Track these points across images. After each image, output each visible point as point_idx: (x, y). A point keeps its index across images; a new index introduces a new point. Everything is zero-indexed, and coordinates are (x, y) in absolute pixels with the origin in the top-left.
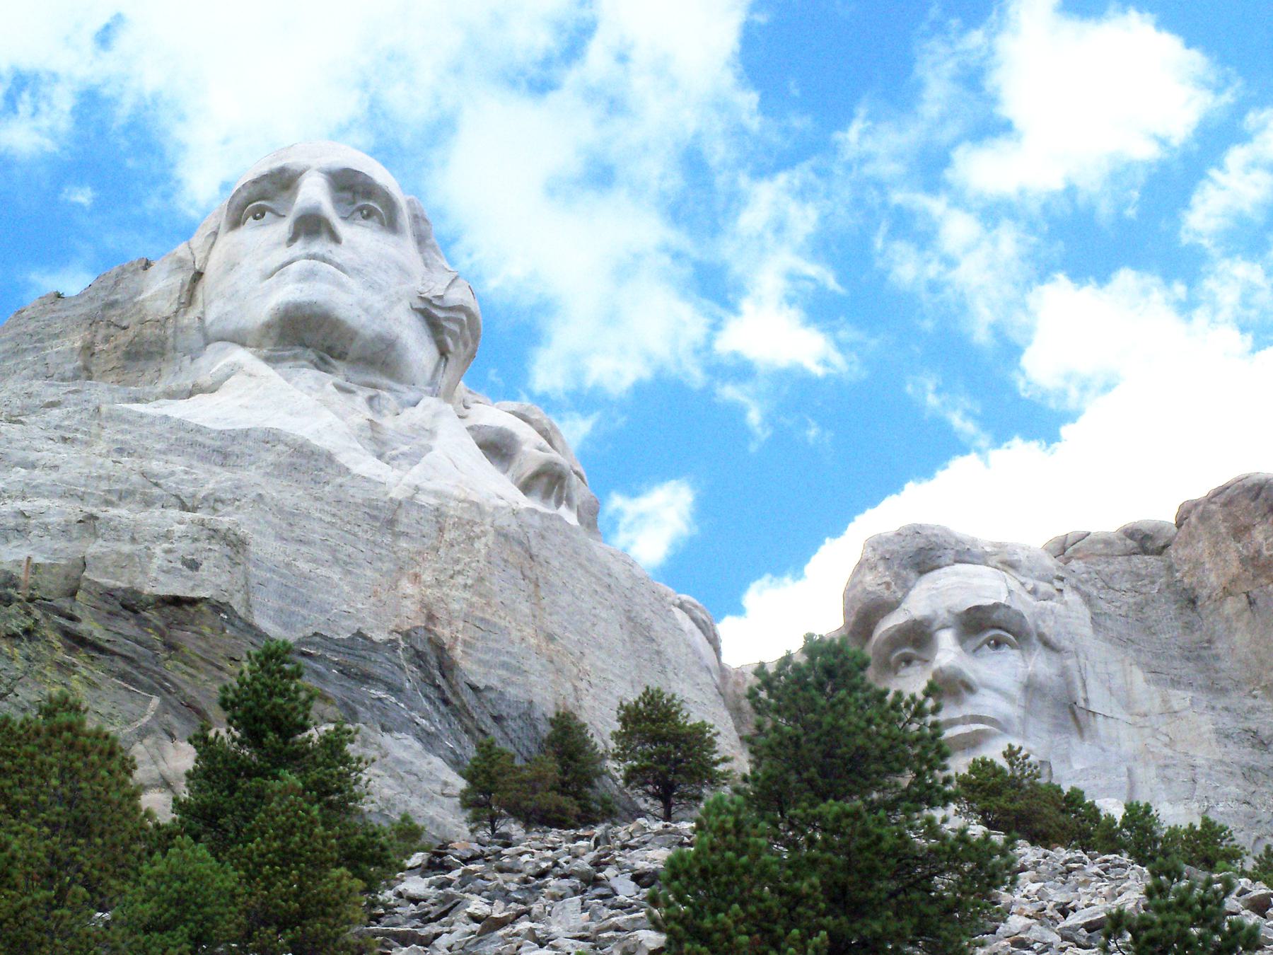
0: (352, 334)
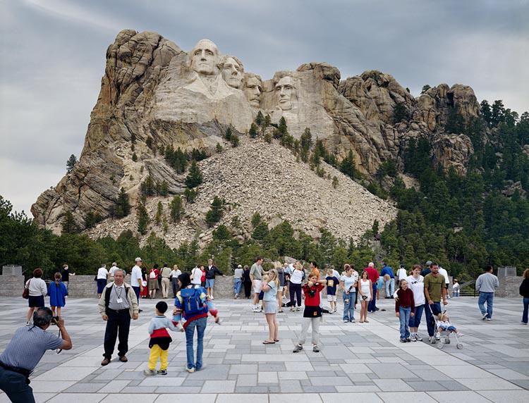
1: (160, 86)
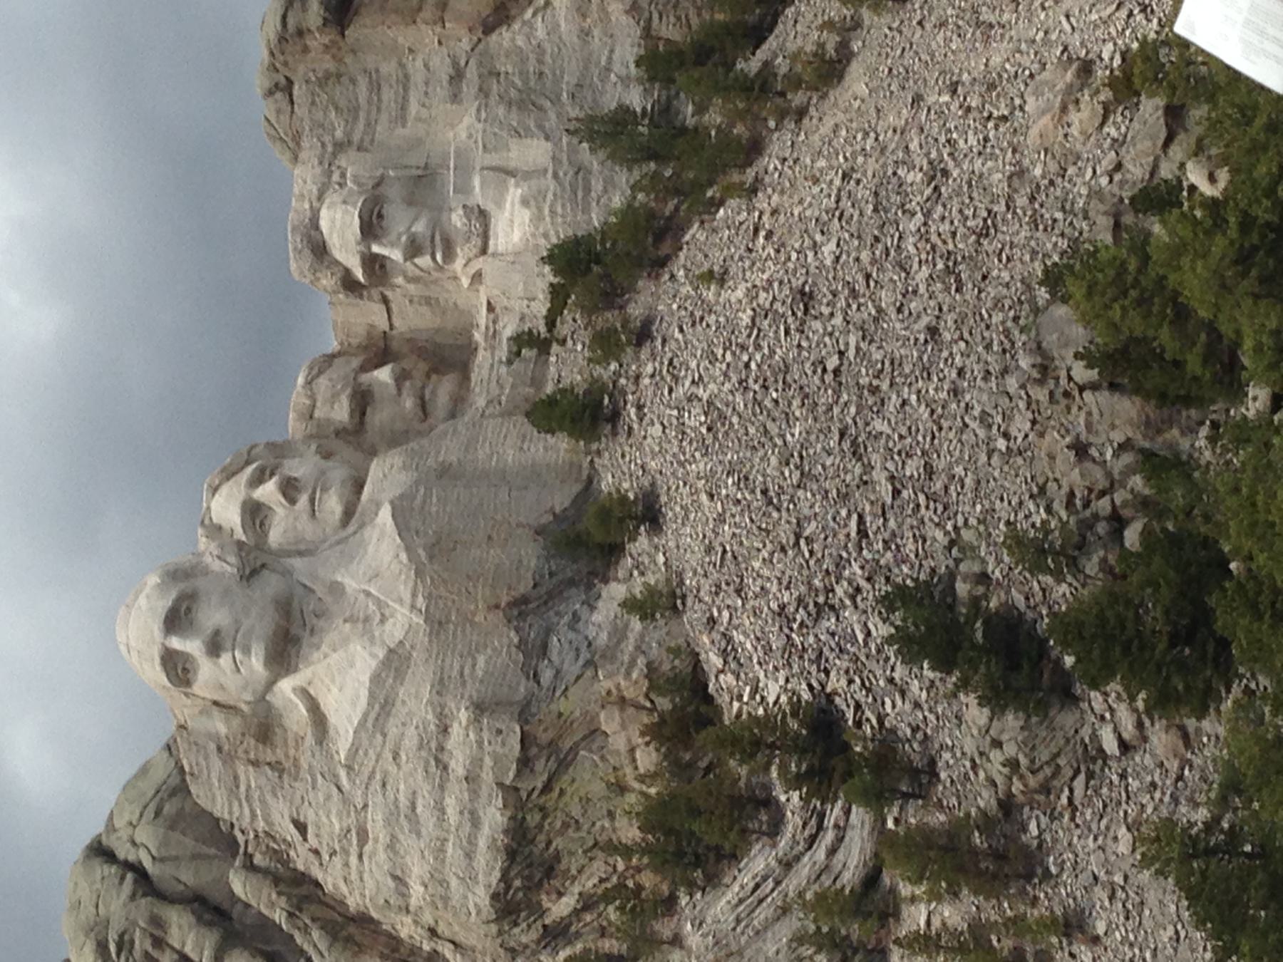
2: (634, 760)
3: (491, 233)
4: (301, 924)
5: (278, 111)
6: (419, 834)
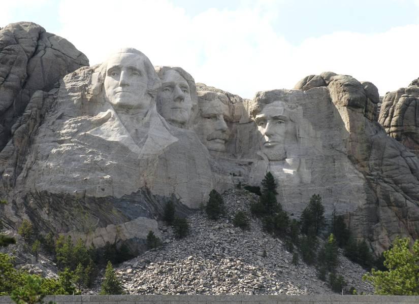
0: (133, 106)
1: (43, 130)
2: (97, 237)
3: (277, 162)
4: (26, 120)
5: (316, 81)
6: (64, 163)
